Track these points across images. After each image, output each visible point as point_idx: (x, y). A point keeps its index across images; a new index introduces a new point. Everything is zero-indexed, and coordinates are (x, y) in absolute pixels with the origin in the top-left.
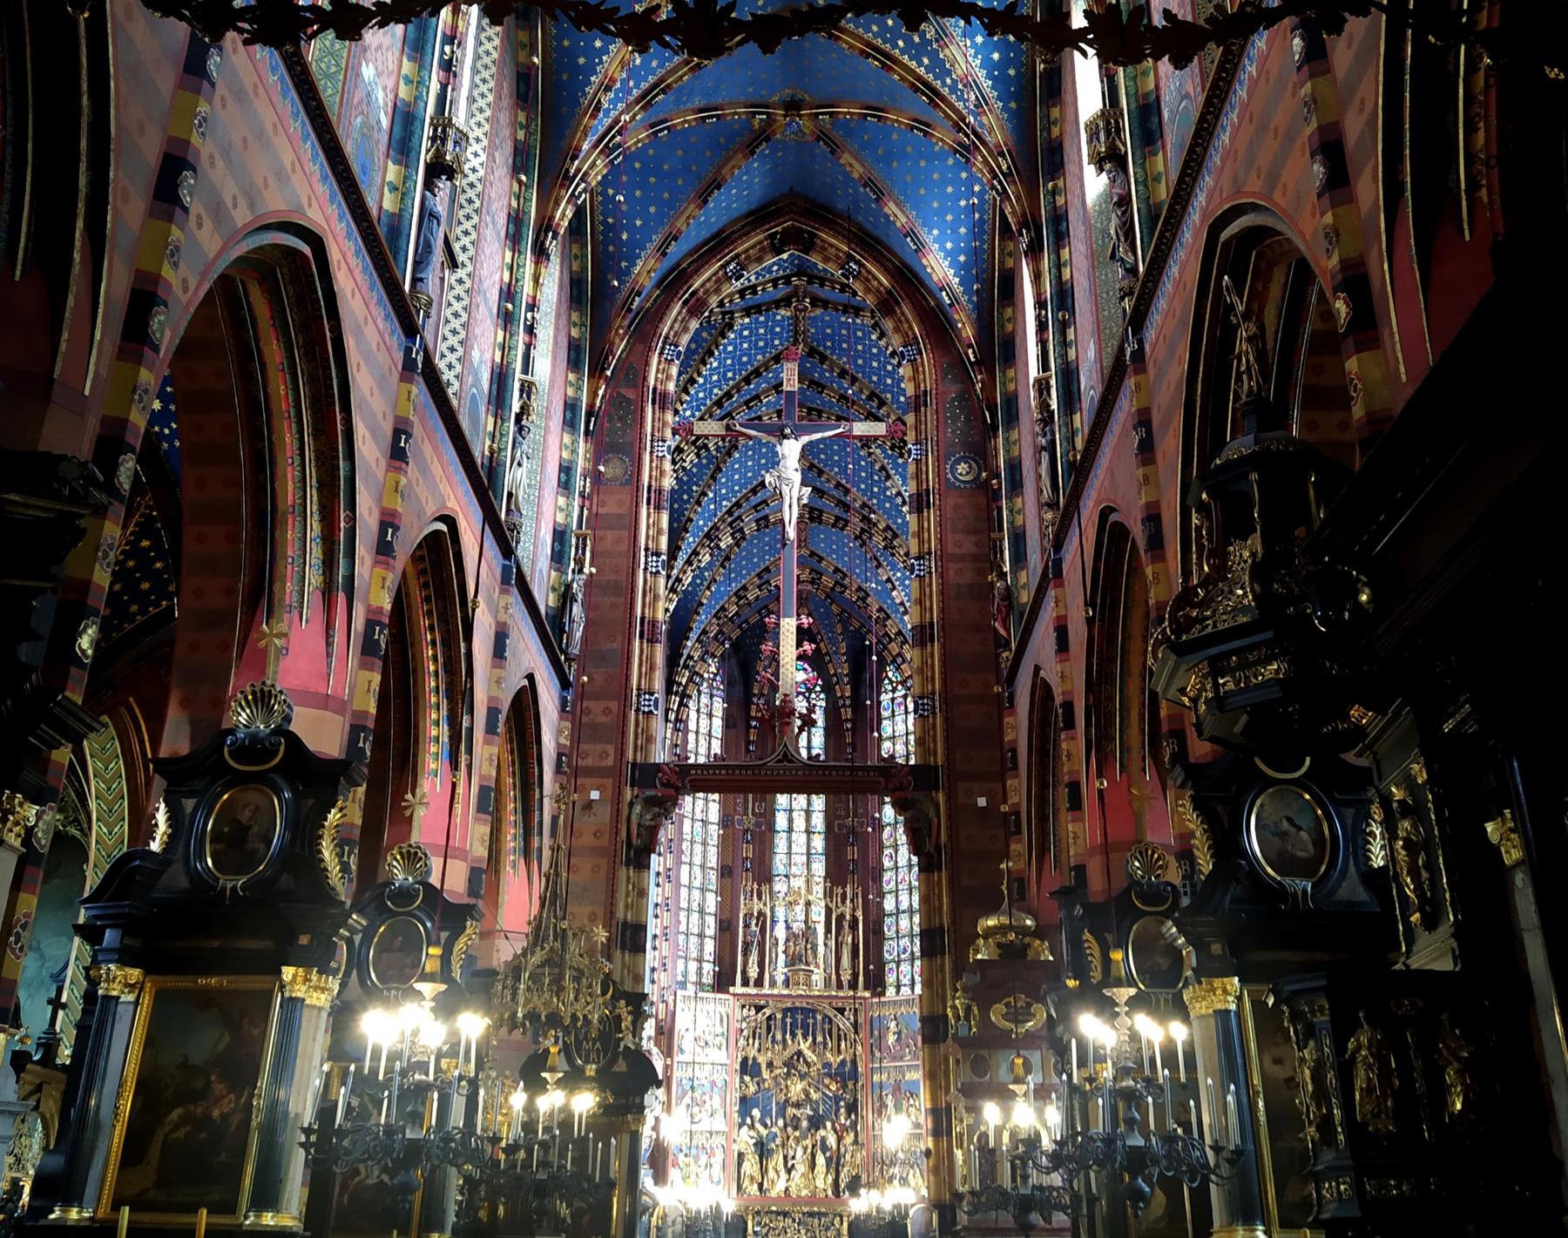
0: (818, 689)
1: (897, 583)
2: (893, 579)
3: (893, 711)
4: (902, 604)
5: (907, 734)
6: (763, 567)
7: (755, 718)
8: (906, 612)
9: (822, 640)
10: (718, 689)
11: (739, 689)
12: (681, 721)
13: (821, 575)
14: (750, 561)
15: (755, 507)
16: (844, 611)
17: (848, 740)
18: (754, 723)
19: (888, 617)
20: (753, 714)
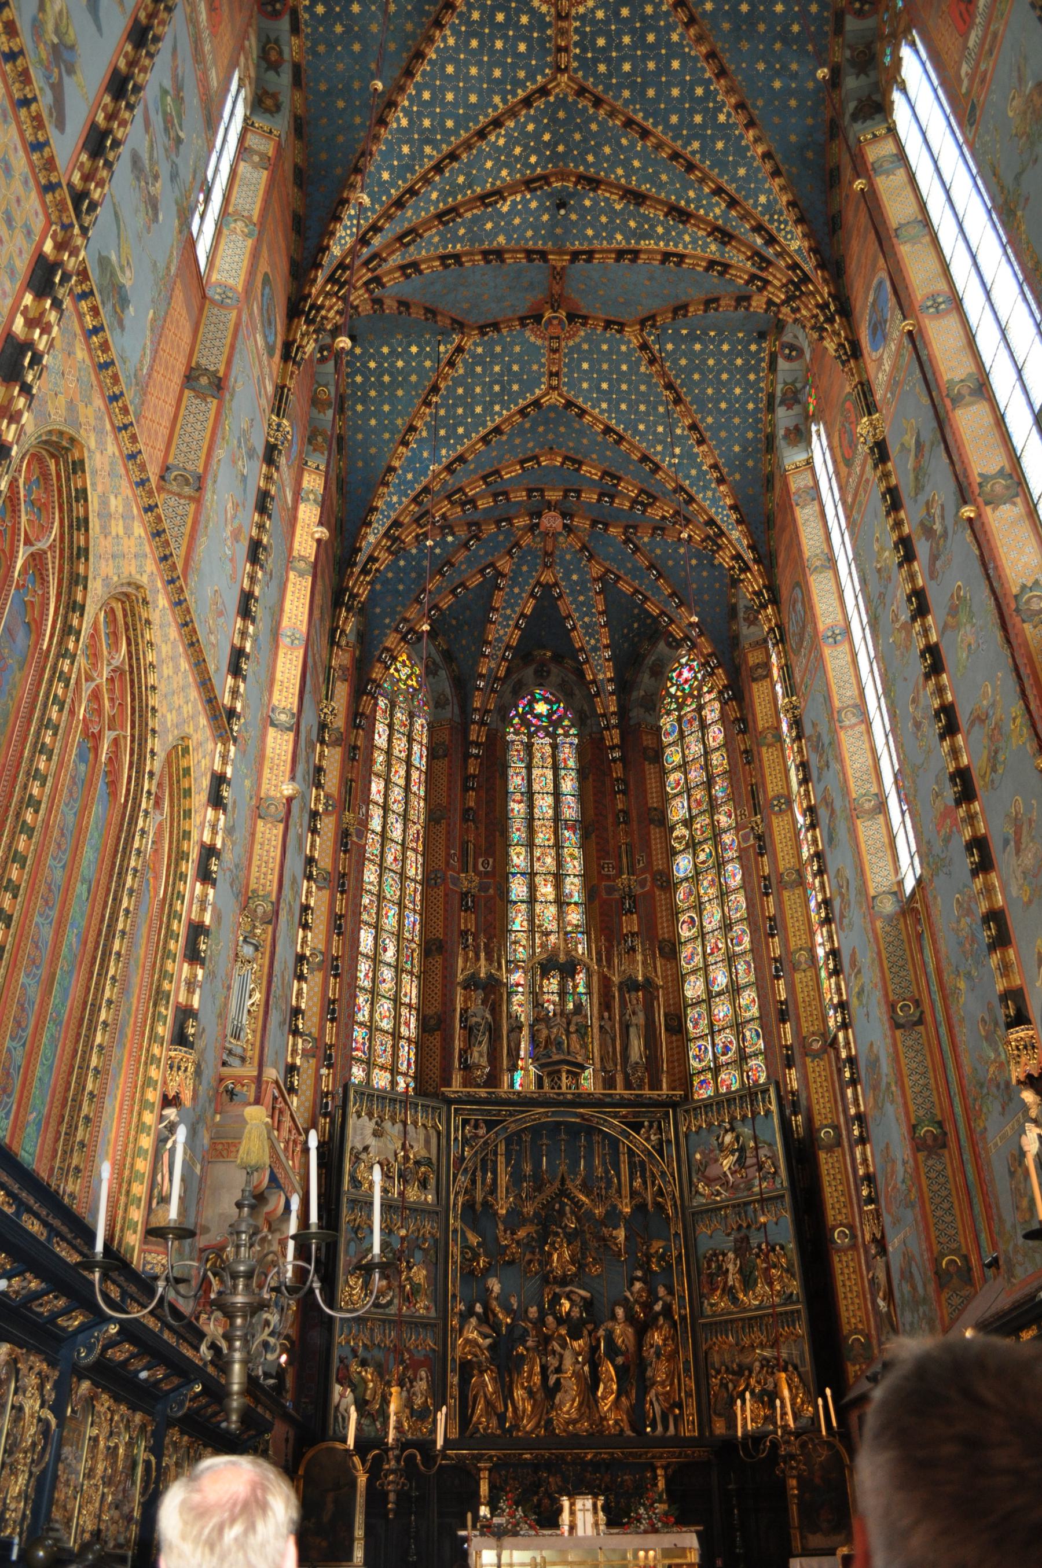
0: (566, 723)
1: (707, 435)
2: (702, 426)
3: (681, 732)
4: (715, 466)
5: (707, 753)
6: (490, 425)
7: (478, 745)
8: (721, 481)
9: (574, 628)
10: (420, 709)
11: (450, 712)
12: (362, 714)
13: (581, 463)
14: (469, 408)
15: (482, 198)
16: (608, 571)
17: (618, 772)
18: (475, 751)
19: (691, 500)
20: (473, 737)
